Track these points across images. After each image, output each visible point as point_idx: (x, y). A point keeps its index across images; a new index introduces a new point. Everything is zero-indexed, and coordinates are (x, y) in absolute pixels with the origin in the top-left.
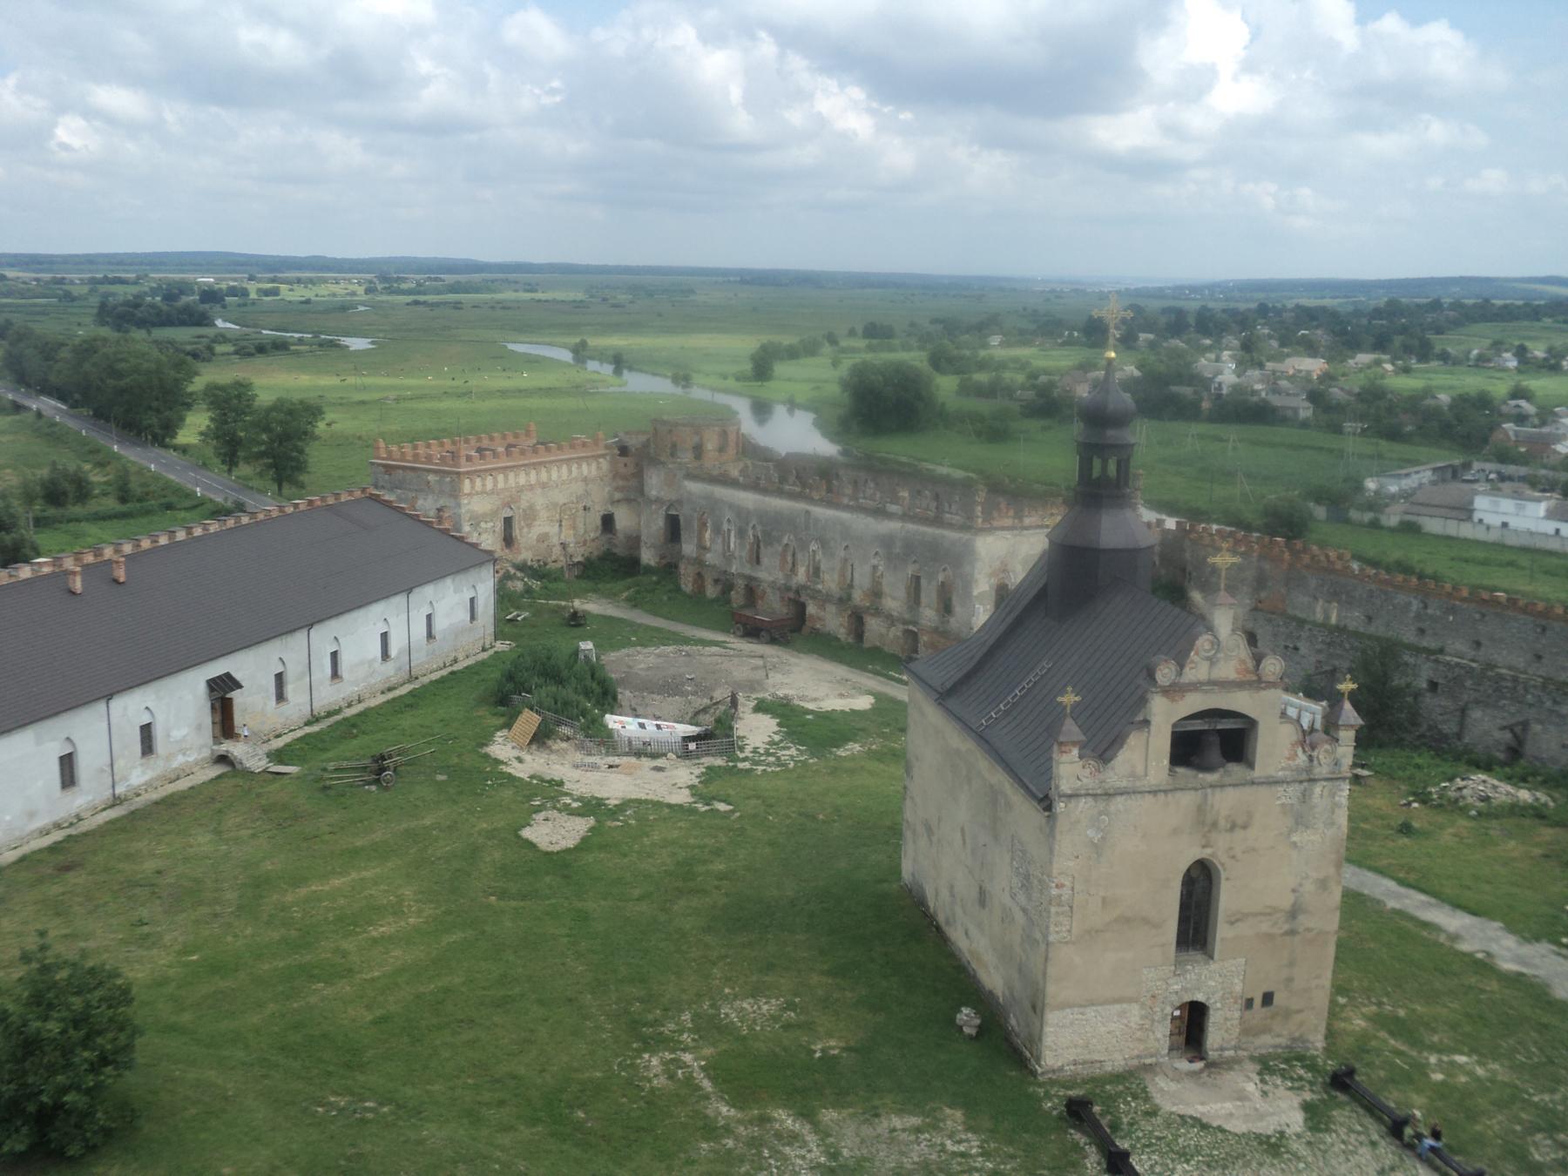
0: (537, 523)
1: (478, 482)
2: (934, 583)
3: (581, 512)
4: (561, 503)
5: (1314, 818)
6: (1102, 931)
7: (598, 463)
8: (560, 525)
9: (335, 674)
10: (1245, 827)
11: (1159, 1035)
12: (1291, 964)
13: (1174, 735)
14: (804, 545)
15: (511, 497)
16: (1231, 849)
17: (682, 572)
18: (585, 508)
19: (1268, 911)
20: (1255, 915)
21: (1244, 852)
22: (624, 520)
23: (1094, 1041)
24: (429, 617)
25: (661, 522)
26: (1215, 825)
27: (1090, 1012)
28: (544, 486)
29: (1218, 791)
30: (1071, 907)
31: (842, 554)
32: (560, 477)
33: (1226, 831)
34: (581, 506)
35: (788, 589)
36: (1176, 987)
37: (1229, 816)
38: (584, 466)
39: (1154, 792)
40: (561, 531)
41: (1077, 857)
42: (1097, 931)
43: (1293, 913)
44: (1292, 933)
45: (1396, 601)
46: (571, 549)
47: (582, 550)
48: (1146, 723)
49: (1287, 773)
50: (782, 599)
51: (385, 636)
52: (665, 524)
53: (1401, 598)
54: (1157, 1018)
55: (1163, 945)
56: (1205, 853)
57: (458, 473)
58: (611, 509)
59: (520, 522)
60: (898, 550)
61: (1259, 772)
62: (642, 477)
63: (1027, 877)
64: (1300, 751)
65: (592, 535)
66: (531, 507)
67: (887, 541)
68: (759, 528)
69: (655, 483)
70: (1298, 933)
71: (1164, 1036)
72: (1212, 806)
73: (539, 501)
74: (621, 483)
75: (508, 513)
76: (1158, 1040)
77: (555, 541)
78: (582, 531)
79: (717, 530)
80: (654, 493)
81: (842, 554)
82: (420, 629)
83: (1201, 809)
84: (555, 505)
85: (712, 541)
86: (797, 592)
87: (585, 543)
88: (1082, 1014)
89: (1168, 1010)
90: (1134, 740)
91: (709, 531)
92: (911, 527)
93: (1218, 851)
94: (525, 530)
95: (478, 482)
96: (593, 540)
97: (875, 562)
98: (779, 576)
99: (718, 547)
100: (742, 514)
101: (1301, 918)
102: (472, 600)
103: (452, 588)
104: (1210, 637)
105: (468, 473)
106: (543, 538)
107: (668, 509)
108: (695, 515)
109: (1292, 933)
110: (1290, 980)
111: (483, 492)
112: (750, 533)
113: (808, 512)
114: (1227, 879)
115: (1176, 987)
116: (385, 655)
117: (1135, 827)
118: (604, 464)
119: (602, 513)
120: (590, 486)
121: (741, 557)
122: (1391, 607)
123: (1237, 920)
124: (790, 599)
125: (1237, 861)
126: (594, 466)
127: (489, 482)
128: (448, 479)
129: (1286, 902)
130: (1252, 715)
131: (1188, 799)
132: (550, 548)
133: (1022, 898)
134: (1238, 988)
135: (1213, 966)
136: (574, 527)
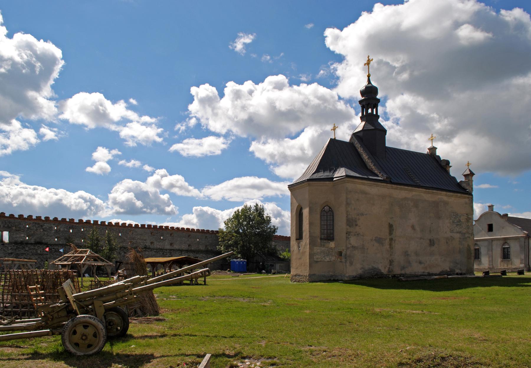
45: (44, 227)
53: (46, 225)
63: (460, 221)
122: (42, 230)
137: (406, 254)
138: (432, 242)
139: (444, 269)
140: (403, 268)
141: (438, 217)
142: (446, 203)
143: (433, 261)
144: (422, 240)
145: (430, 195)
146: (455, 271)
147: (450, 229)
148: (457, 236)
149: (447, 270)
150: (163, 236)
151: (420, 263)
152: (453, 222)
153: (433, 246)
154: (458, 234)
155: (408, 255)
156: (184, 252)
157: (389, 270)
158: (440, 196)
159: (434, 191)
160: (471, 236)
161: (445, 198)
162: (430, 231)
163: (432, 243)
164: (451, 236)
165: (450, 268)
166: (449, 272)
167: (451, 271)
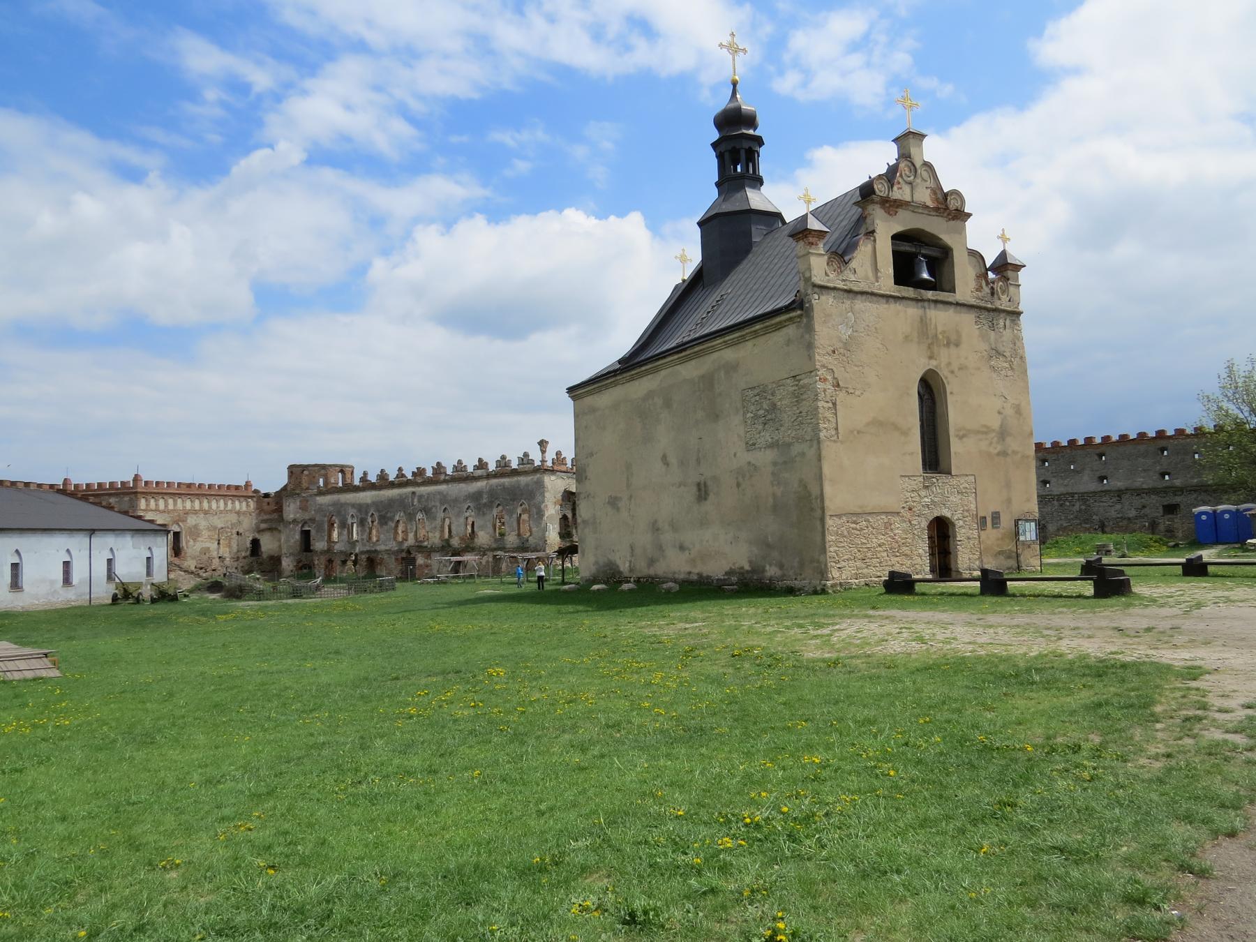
0: (200, 539)
1: (152, 502)
2: (515, 516)
3: (235, 535)
4: (219, 526)
6: (863, 433)
7: (248, 503)
8: (219, 544)
9: (16, 585)
10: (957, 345)
11: (921, 551)
12: (1008, 485)
13: (893, 251)
14: (411, 517)
15: (179, 515)
16: (949, 364)
17: (316, 562)
18: (238, 533)
19: (984, 430)
20: (978, 432)
21: (960, 369)
22: (268, 544)
23: (869, 555)
24: (110, 561)
25: (298, 536)
26: (936, 335)
28: (206, 513)
29: (932, 305)
30: (834, 404)
31: (442, 515)
32: (218, 507)
33: (944, 345)
34: (234, 531)
35: (403, 551)
36: (926, 500)
38: (237, 503)
39: (888, 298)
40: (219, 548)
41: (834, 352)
42: (859, 432)
43: (1003, 434)
44: (1003, 454)
46: (228, 561)
47: (236, 564)
48: (873, 232)
49: (978, 301)
50: (397, 559)
51: (67, 565)
52: (301, 538)
54: (915, 532)
56: (932, 364)
57: (136, 493)
58: (257, 536)
59: (186, 537)
60: (485, 501)
62: (282, 511)
64: (984, 283)
65: (243, 554)
66: (196, 526)
67: (476, 496)
68: (376, 516)
69: (291, 510)
70: (1007, 454)
72: (930, 319)
73: (203, 524)
74: (265, 517)
75: (177, 529)
76: (920, 556)
77: (215, 554)
78: (235, 550)
79: (343, 525)
80: (292, 516)
81: (442, 515)
82: (100, 569)
83: (923, 321)
84: (215, 528)
85: (340, 534)
86: (409, 552)
87: (238, 559)
88: (855, 522)
89: (925, 524)
90: (864, 249)
91: (336, 530)
92: (494, 481)
93: (943, 362)
94: (191, 542)
95: (152, 502)
96: (244, 558)
97: (467, 514)
98: (393, 546)
99: (345, 537)
100: (362, 508)
101: (1008, 440)
102: (148, 559)
103: (131, 544)
104: (910, 164)
105: (143, 493)
106: (205, 551)
107: (303, 526)
108: (326, 519)
110: (1009, 501)
111: (156, 510)
112: (370, 520)
113: (414, 493)
114: (951, 393)
115: (926, 500)
116: (67, 580)
117: (876, 328)
118: (252, 504)
119: (251, 539)
120: (242, 517)
121: (363, 539)
124: (403, 559)
126: (244, 504)
127: (161, 503)
128: (127, 499)
129: (995, 423)
130: (947, 239)
131: (913, 311)
132: (211, 559)
133: (766, 437)
134: (973, 506)
135: (954, 481)
136: (230, 546)
137: (655, 528)
138: (703, 489)
139: (734, 564)
140: (652, 562)
141: (714, 416)
142: (732, 368)
143: (707, 541)
144: (682, 487)
145: (693, 362)
146: (764, 571)
147: (747, 443)
148: (765, 458)
149: (742, 568)
150: (1073, 462)
151: (682, 548)
152: (756, 417)
153: (706, 499)
154: (768, 452)
155: (658, 530)
156: (1127, 496)
157: (630, 566)
158: (716, 355)
159: (696, 349)
160: (811, 446)
161: (729, 355)
162: (698, 461)
163: (702, 492)
164: (749, 463)
165: (750, 562)
166: (747, 571)
167: (753, 571)
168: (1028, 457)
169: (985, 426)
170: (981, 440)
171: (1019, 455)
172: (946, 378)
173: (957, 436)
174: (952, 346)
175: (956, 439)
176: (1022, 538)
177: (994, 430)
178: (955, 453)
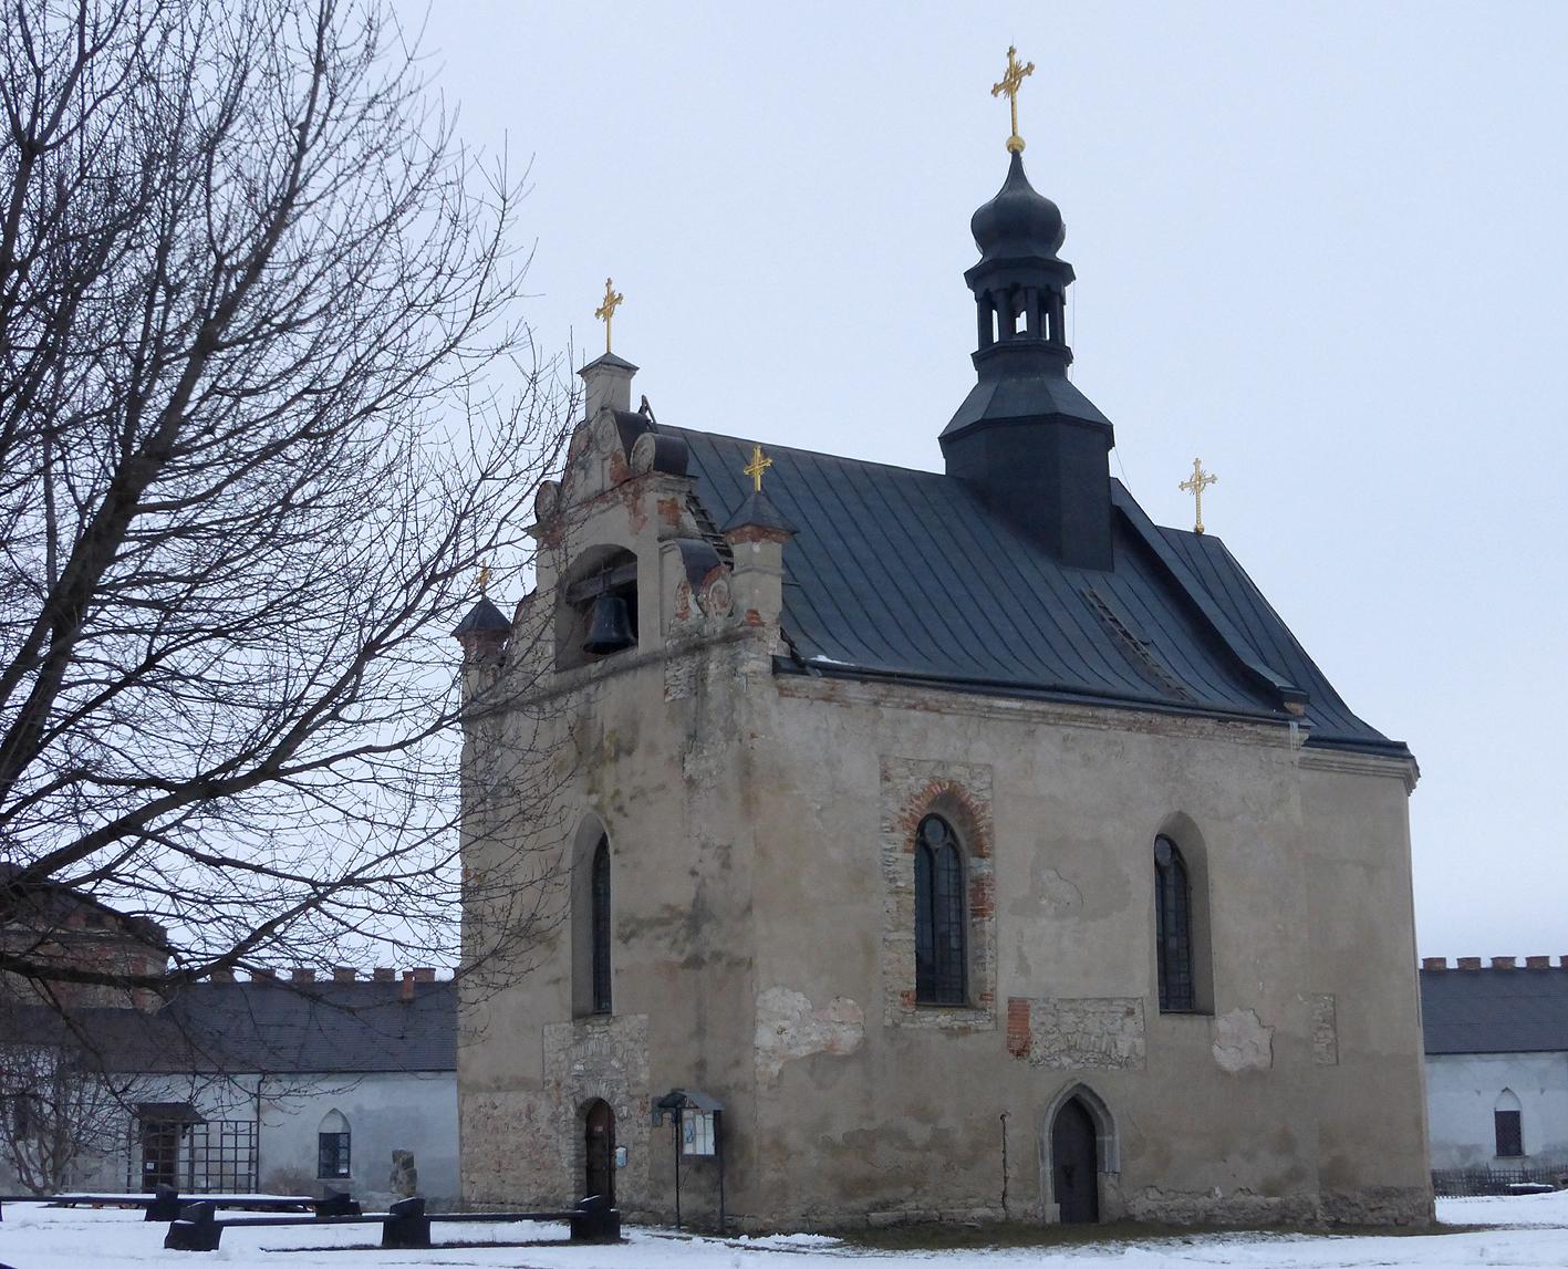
5: (710, 721)
10: (630, 752)
16: (617, 793)
21: (631, 799)
26: (600, 747)
27: (499, 1098)
33: (611, 759)
36: (578, 1067)
37: (614, 732)
43: (697, 917)
44: (695, 962)
55: (557, 981)
61: (644, 647)
70: (703, 961)
71: (570, 1165)
89: (572, 1110)
101: (706, 928)
109: (695, 962)
110: (701, 1065)
114: (616, 852)
123: (633, 934)
125: (626, 815)
134: (644, 1076)
135: (615, 1028)
168: (739, 963)
169: (668, 907)
170: (658, 938)
171: (724, 962)
172: (609, 823)
173: (620, 937)
174: (622, 755)
175: (619, 942)
176: (688, 1149)
177: (681, 914)
178: (617, 972)
